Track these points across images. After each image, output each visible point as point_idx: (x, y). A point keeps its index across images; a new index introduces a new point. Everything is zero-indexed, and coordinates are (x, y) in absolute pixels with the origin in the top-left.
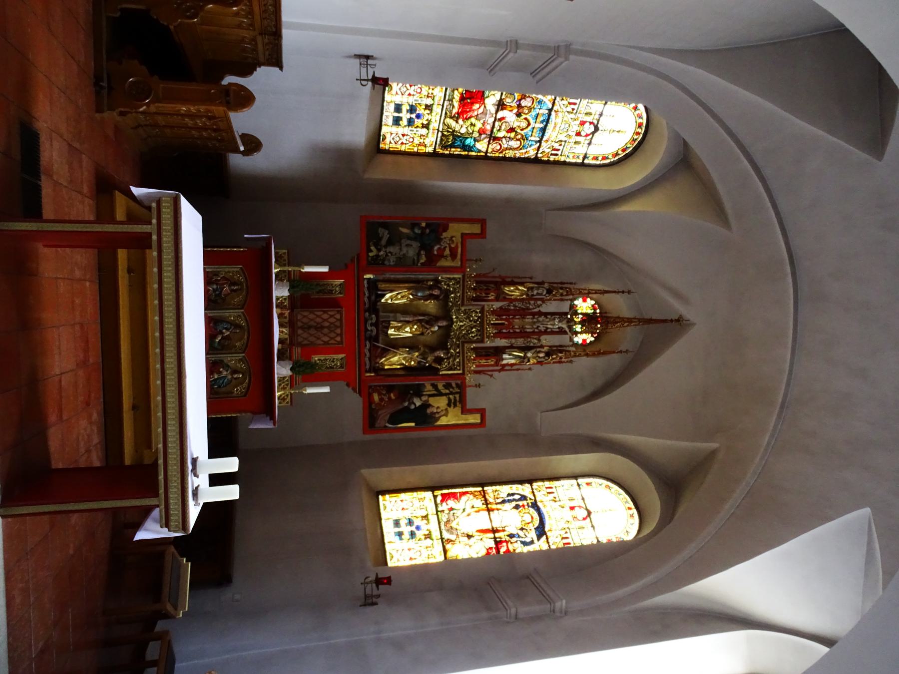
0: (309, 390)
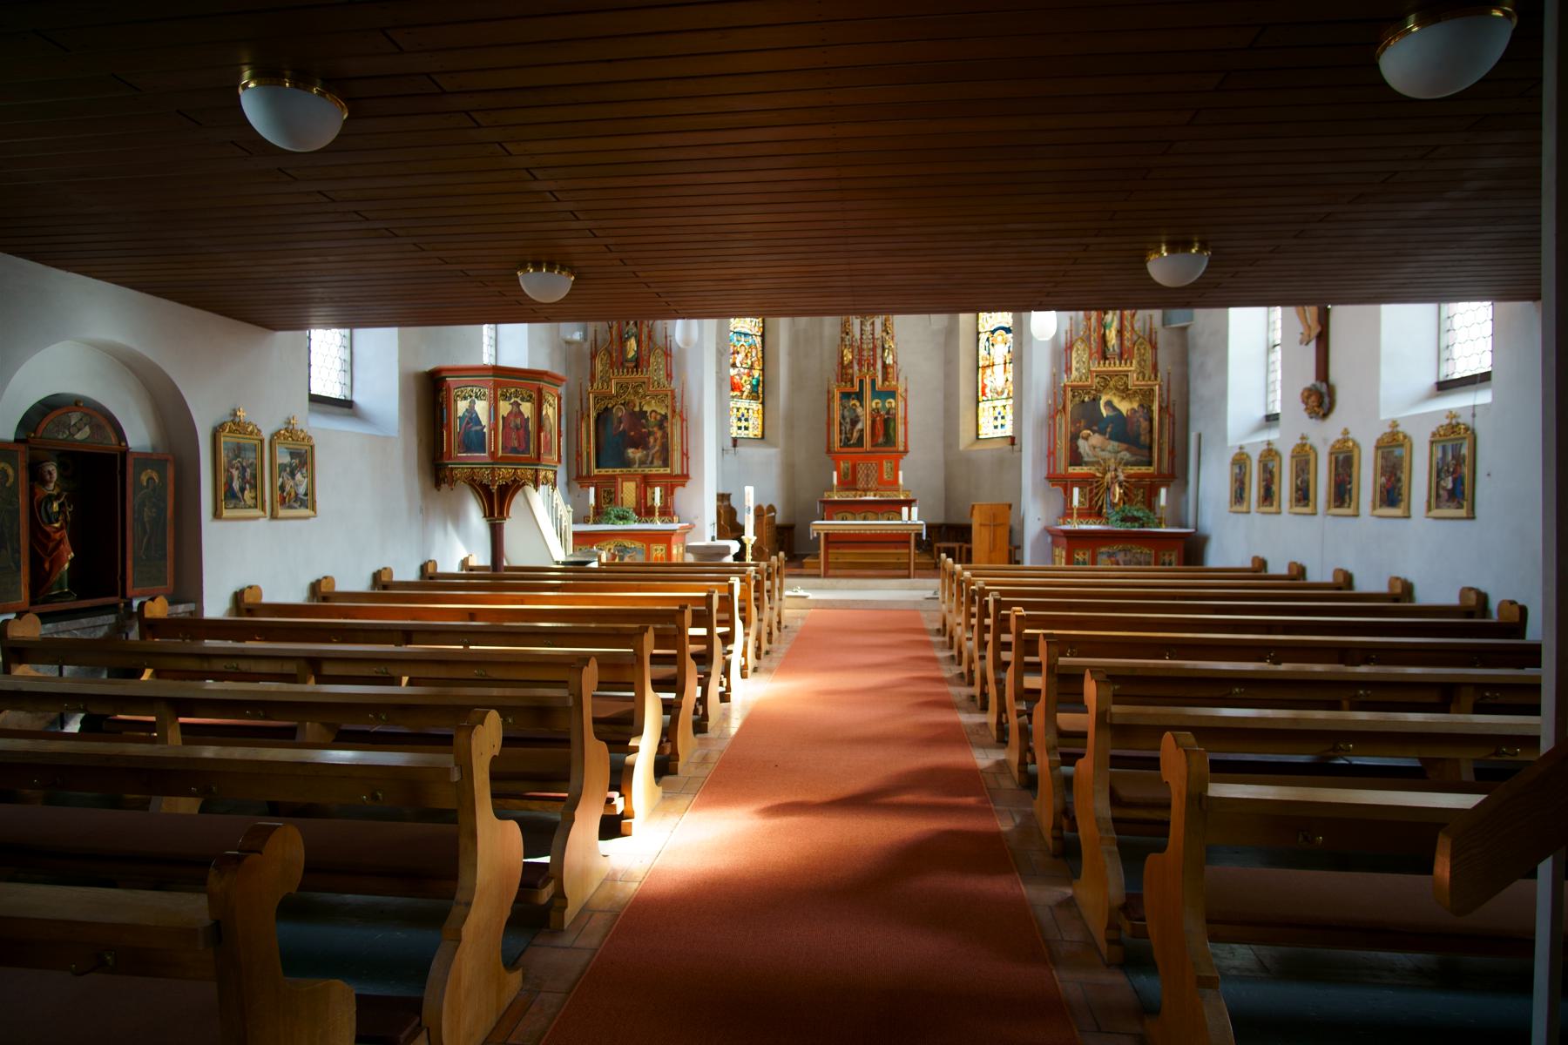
0: (901, 481)
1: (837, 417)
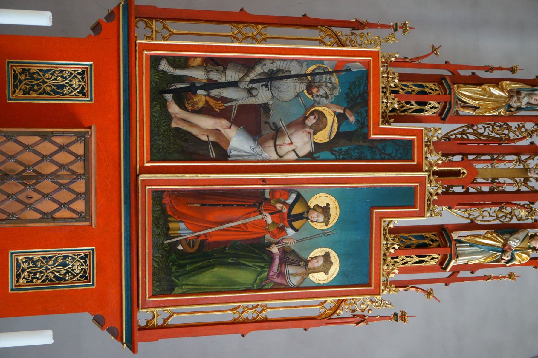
1: (278, 49)
